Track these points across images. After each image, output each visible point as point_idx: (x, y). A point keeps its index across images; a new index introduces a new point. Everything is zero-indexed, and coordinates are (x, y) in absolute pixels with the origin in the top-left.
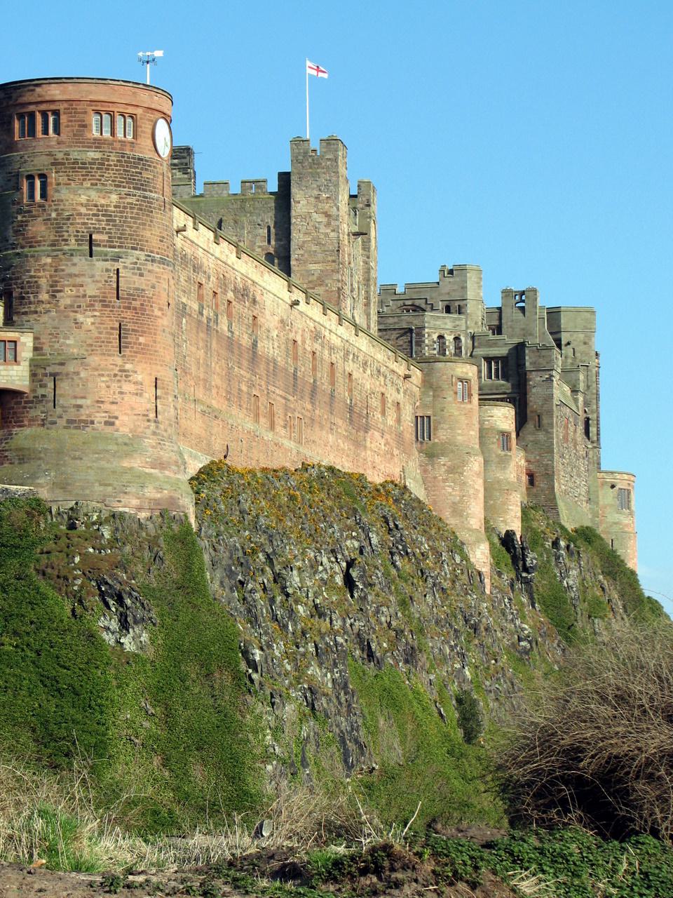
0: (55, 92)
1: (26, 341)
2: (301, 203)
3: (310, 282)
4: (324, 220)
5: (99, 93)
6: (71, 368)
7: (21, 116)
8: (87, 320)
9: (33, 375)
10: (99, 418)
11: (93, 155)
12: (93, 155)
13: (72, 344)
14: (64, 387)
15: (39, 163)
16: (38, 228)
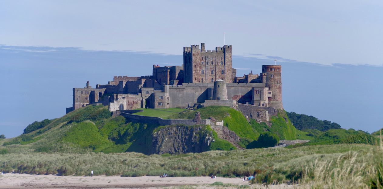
0: (274, 66)
1: (272, 92)
2: (227, 55)
4: (230, 57)
5: (278, 67)
6: (276, 95)
7: (270, 68)
8: (277, 90)
9: (272, 96)
10: (278, 100)
11: (277, 73)
12: (277, 73)
13: (276, 92)
14: (275, 97)
15: (272, 74)
16: (272, 80)
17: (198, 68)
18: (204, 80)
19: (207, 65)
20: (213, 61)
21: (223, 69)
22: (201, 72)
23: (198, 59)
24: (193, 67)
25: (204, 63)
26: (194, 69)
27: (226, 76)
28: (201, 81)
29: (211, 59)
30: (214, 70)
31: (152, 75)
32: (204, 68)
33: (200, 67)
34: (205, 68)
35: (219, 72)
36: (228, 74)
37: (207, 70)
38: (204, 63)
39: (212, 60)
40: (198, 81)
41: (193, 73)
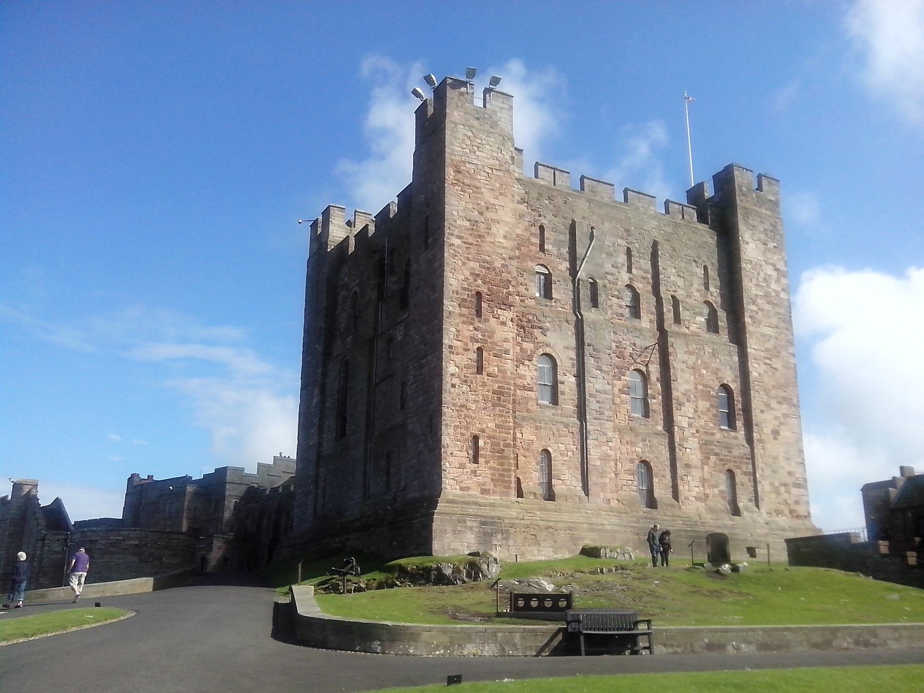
3: (767, 350)
4: (774, 274)
17: (503, 329)
18: (567, 480)
19: (590, 315)
20: (638, 286)
21: (731, 378)
22: (531, 373)
23: (499, 231)
24: (450, 305)
25: (562, 293)
26: (456, 333)
27: (758, 451)
28: (533, 480)
29: (622, 258)
30: (655, 370)
31: (117, 513)
32: (561, 343)
33: (526, 326)
34: (572, 341)
35: (703, 405)
36: (776, 433)
37: (590, 362)
38: (562, 293)
39: (625, 277)
40: (500, 479)
41: (447, 381)
